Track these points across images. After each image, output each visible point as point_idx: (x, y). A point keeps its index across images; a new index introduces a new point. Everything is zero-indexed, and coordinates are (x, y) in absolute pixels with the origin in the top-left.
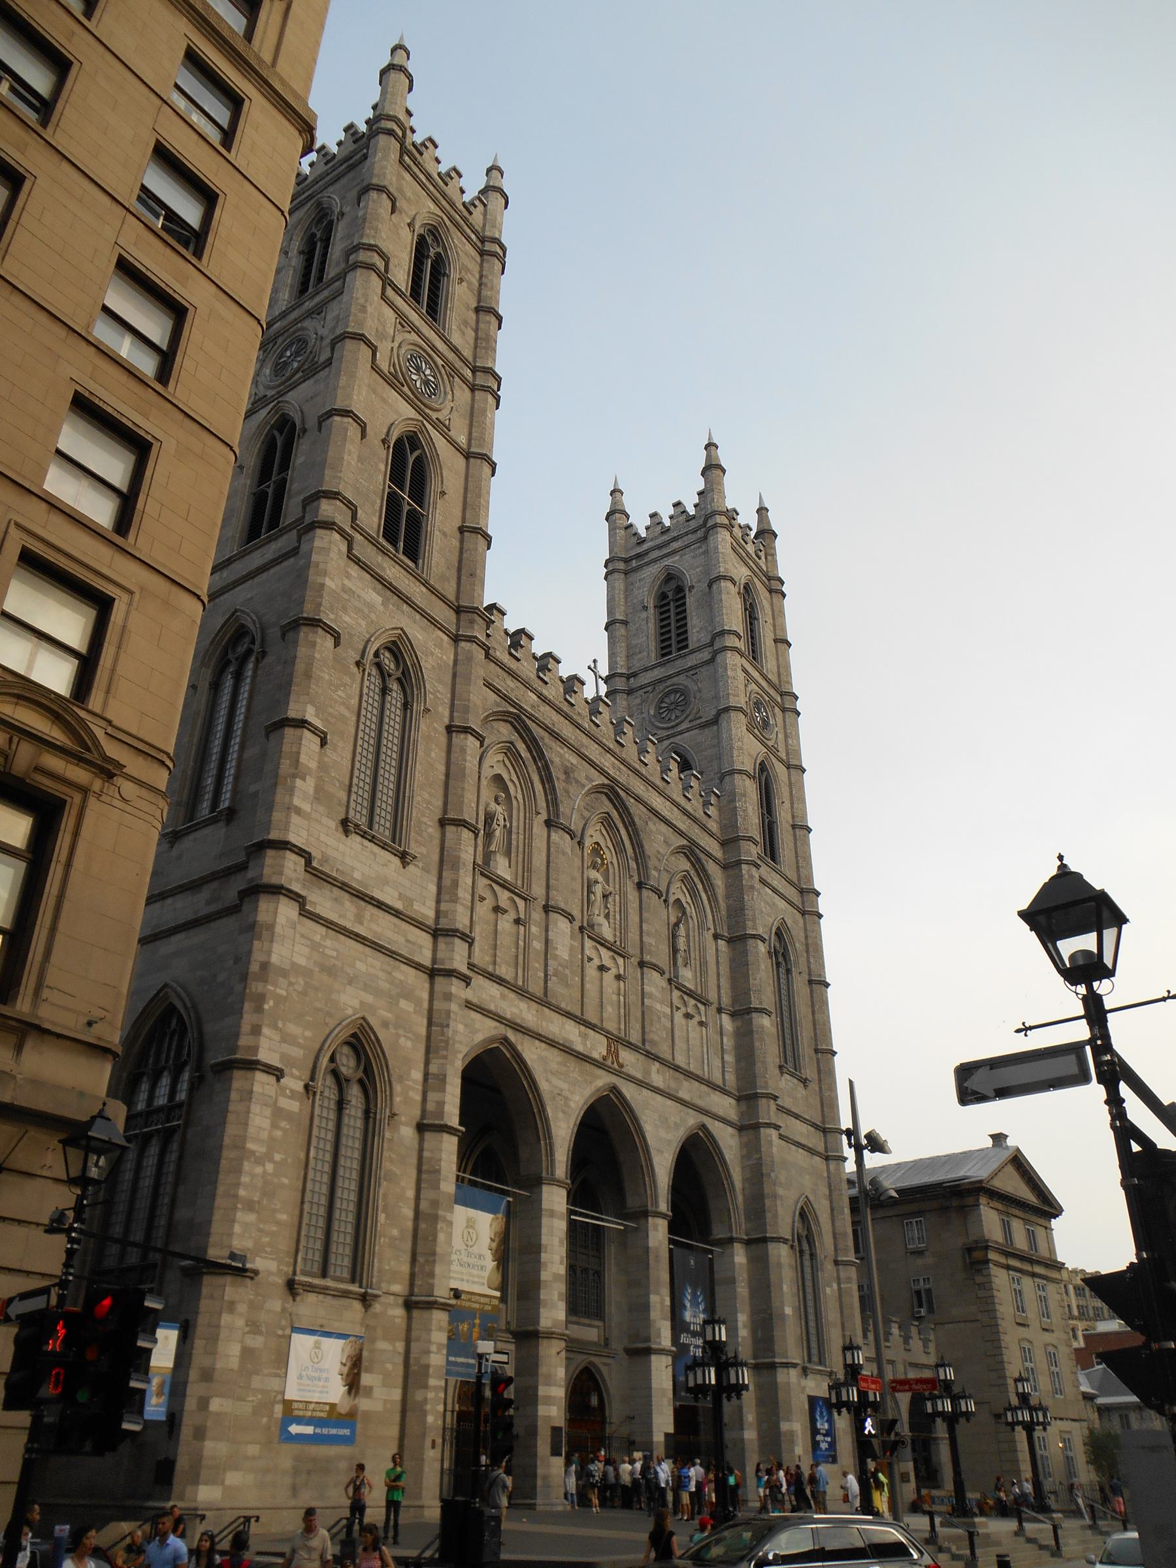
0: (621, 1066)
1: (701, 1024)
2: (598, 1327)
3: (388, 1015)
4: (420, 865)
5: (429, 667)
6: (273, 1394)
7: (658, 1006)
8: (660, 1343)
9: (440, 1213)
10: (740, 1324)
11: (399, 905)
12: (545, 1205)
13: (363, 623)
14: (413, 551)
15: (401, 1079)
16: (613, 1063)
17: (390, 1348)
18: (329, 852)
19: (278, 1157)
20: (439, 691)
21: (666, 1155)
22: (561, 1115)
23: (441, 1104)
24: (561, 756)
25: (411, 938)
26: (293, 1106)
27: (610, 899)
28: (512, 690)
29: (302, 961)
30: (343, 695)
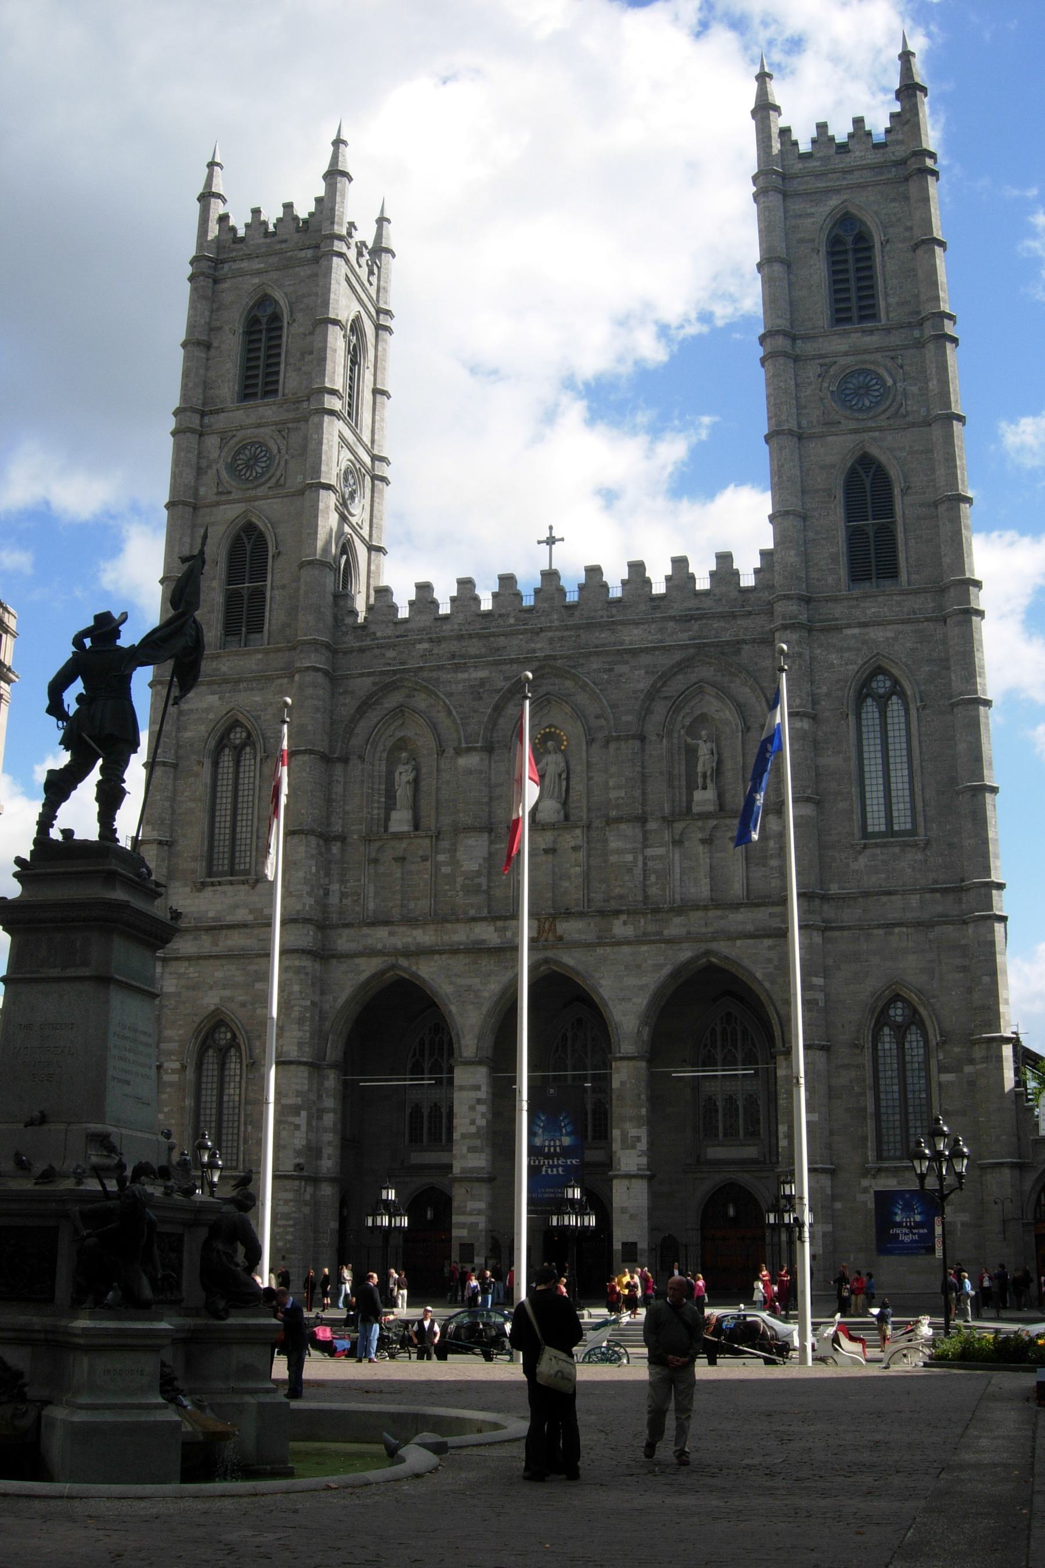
0: (561, 938)
2: (756, 1145)
7: (629, 858)
8: (619, 1170)
9: (283, 1118)
10: (781, 1135)
11: (250, 918)
12: (457, 1082)
13: (203, 728)
14: (256, 625)
16: (546, 940)
19: (166, 1110)
21: (639, 1000)
22: (471, 1007)
24: (464, 680)
26: (175, 1078)
28: (394, 659)
30: (186, 794)
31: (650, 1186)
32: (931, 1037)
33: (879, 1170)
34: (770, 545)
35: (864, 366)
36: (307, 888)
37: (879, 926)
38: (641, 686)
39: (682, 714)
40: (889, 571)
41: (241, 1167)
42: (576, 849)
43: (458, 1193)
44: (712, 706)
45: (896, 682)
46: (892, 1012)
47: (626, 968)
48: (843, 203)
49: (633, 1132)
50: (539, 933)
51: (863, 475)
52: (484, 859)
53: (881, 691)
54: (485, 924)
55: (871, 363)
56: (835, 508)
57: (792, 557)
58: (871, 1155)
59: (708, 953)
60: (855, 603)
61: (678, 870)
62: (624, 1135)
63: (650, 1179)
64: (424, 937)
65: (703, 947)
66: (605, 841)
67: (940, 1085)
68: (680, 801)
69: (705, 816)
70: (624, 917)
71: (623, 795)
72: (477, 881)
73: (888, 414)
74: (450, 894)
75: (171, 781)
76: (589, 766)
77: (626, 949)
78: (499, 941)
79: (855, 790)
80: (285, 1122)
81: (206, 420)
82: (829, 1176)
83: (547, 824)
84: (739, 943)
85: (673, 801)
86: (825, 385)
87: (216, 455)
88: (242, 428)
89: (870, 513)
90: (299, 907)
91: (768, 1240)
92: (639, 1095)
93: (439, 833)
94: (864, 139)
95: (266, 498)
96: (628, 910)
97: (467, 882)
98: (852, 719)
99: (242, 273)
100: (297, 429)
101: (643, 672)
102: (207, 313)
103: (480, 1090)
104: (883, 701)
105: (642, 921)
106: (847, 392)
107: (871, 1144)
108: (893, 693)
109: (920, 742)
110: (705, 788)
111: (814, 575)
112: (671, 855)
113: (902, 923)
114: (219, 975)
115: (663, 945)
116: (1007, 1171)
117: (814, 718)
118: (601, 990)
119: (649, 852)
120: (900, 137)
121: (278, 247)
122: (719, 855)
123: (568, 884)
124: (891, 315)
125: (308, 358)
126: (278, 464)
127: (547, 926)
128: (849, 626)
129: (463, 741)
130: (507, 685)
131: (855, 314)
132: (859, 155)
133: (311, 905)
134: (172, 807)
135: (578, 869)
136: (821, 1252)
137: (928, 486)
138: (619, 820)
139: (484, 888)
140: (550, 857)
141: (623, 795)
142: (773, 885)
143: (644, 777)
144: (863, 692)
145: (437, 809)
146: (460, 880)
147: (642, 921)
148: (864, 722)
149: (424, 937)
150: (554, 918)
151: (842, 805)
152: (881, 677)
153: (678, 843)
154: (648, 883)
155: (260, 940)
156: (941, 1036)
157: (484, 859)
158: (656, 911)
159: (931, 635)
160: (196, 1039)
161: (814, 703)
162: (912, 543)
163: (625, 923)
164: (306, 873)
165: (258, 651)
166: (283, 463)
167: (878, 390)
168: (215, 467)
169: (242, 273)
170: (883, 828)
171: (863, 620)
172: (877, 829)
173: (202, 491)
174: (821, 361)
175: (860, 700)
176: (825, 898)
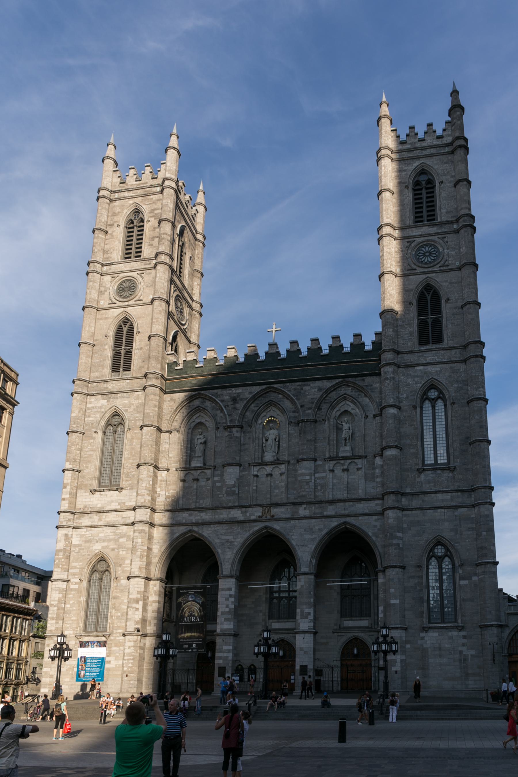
0: (273, 516)
1: (358, 469)
3: (115, 546)
4: (129, 488)
5: (131, 410)
7: (308, 477)
9: (129, 605)
10: (380, 612)
11: (118, 507)
13: (98, 416)
15: (120, 565)
16: (266, 517)
17: (118, 649)
18: (87, 504)
19: (71, 602)
20: (137, 417)
21: (310, 546)
22: (228, 550)
23: (131, 569)
25: (124, 516)
26: (77, 586)
27: (277, 440)
29: (77, 543)
31: (315, 637)
32: (456, 562)
33: (430, 628)
34: (379, 329)
35: (429, 242)
36: (147, 492)
37: (430, 508)
38: (315, 397)
39: (335, 410)
40: (438, 338)
41: (108, 630)
42: (282, 474)
43: (219, 641)
44: (350, 407)
45: (440, 392)
46: (436, 551)
47: (305, 530)
48: (421, 164)
49: (307, 610)
50: (262, 514)
51: (427, 295)
53: (433, 397)
54: (236, 509)
55: (432, 241)
56: (413, 310)
57: (390, 332)
58: (425, 620)
59: (345, 523)
60: (421, 354)
61: (331, 484)
62: (302, 612)
63: (315, 633)
64: (206, 516)
65: (343, 520)
66: (296, 470)
67: (460, 586)
68: (333, 451)
69: (345, 458)
70: (304, 506)
71: (305, 448)
72: (233, 489)
73: (439, 265)
74: (220, 496)
75: (81, 441)
76: (289, 433)
77: (305, 521)
78: (243, 518)
79: (419, 443)
80: (131, 607)
81: (105, 268)
82: (404, 631)
83: (268, 462)
84: (360, 518)
85: (330, 451)
86: (409, 251)
87: (109, 285)
88: (122, 272)
89: (429, 313)
90: (143, 501)
91: (373, 658)
92: (310, 592)
93: (215, 467)
94: (433, 134)
95: (133, 306)
96: (306, 502)
97: (228, 489)
98: (418, 410)
99: (125, 198)
100: (150, 273)
101: (316, 390)
102: (106, 217)
103: (231, 590)
104: (433, 402)
105: (313, 508)
106: (420, 255)
107: (425, 615)
108: (439, 398)
109: (452, 420)
110: (346, 445)
111: (401, 341)
112: (328, 476)
113: (442, 507)
114: (101, 535)
115: (323, 519)
116: (494, 628)
117: (399, 408)
118: (292, 541)
119: (317, 475)
120: (450, 133)
121: (142, 185)
122: (352, 477)
123: (277, 491)
124: (443, 218)
125: (157, 240)
126: (140, 290)
127: (266, 511)
128: (417, 365)
129: (228, 422)
130: (251, 396)
131: (425, 218)
132: (430, 141)
133: (148, 500)
134: (81, 453)
135: (283, 484)
136: (400, 669)
137: (458, 299)
138: (303, 460)
139: (237, 492)
140: (269, 478)
141: (305, 448)
142: (378, 490)
143: (315, 440)
144: (424, 398)
145: (214, 455)
146: (225, 489)
147: (313, 508)
148: (424, 412)
149: (206, 516)
150: (270, 507)
151: (412, 451)
152: (433, 390)
153: (332, 471)
155: (123, 518)
156: (461, 562)
158: (321, 502)
159: (459, 370)
160: (88, 566)
161: (400, 402)
162: (450, 326)
163: (305, 509)
165: (127, 379)
166: (142, 289)
167: (435, 254)
168: (108, 291)
169: (125, 198)
170: (433, 462)
171: (425, 362)
172: (429, 462)
173: (102, 303)
174: (408, 240)
175: (422, 401)
176: (403, 494)
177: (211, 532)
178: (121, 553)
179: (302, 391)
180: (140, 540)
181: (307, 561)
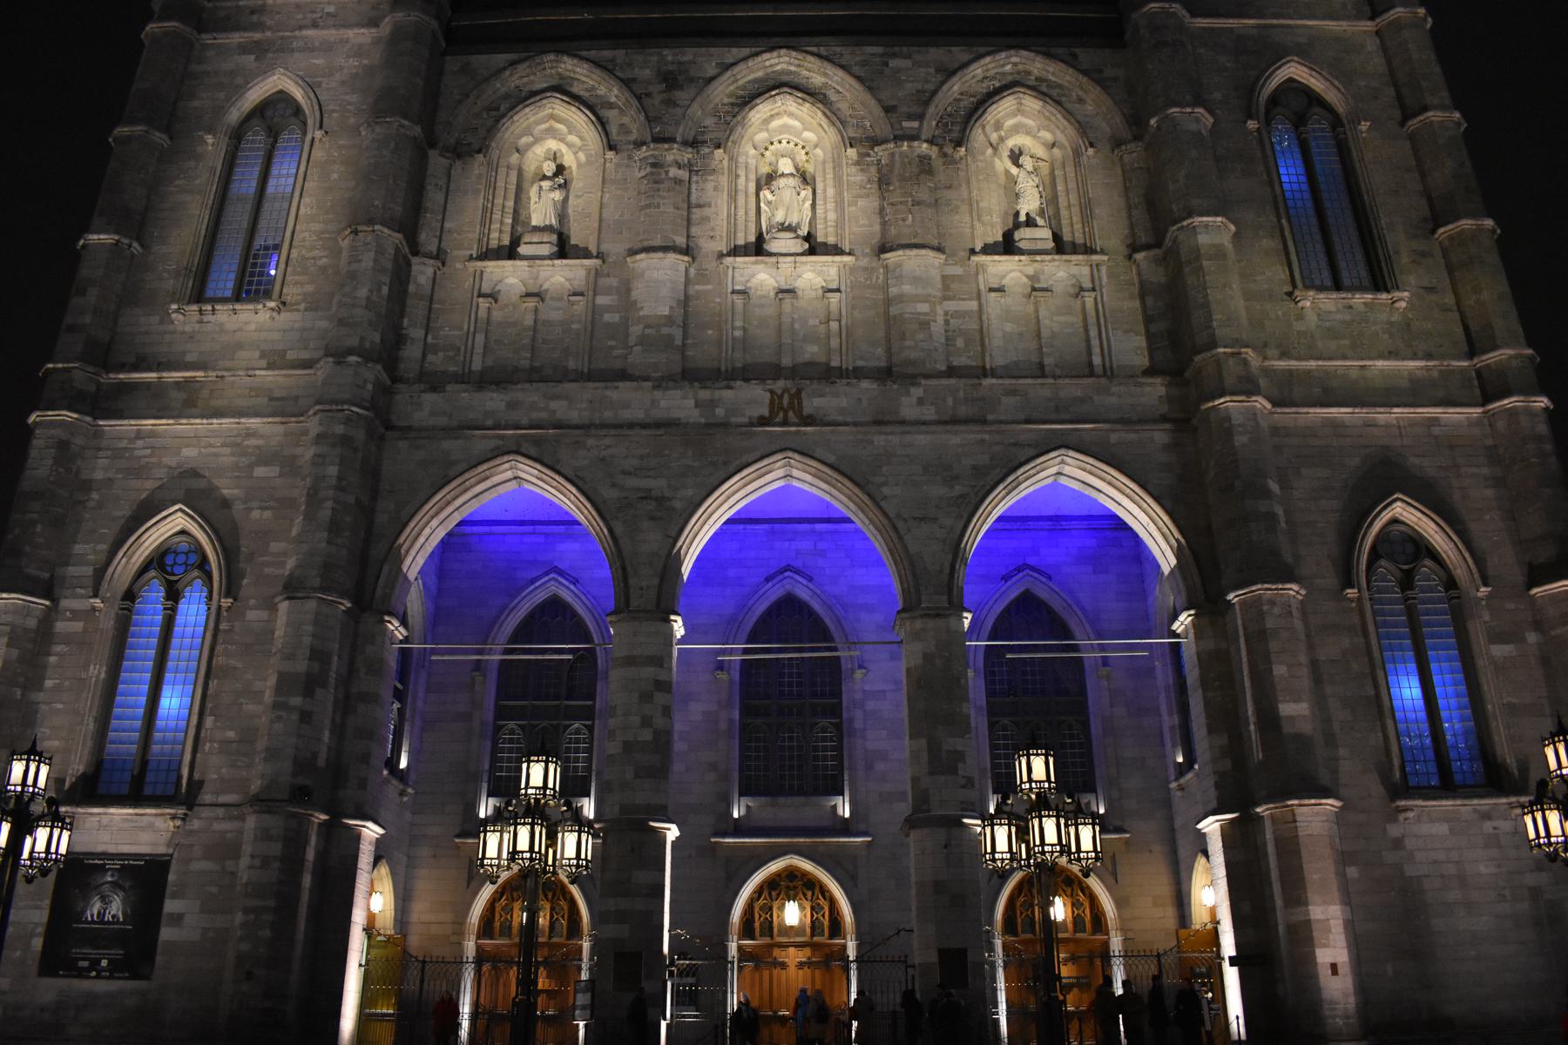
4: (302, 307)
5: (333, 85)
6: (32, 925)
7: (923, 308)
26: (78, 626)
50: (771, 412)
52: (679, 301)
72: (665, 331)
77: (921, 439)
97: (648, 331)
101: (932, 70)
119: (952, 306)
139: (678, 342)
146: (636, 330)
154: (951, 349)
157: (679, 301)
164: (371, 291)
177: (586, 462)
178: (256, 514)
179: (887, 71)
180: (333, 471)
181: (941, 571)
